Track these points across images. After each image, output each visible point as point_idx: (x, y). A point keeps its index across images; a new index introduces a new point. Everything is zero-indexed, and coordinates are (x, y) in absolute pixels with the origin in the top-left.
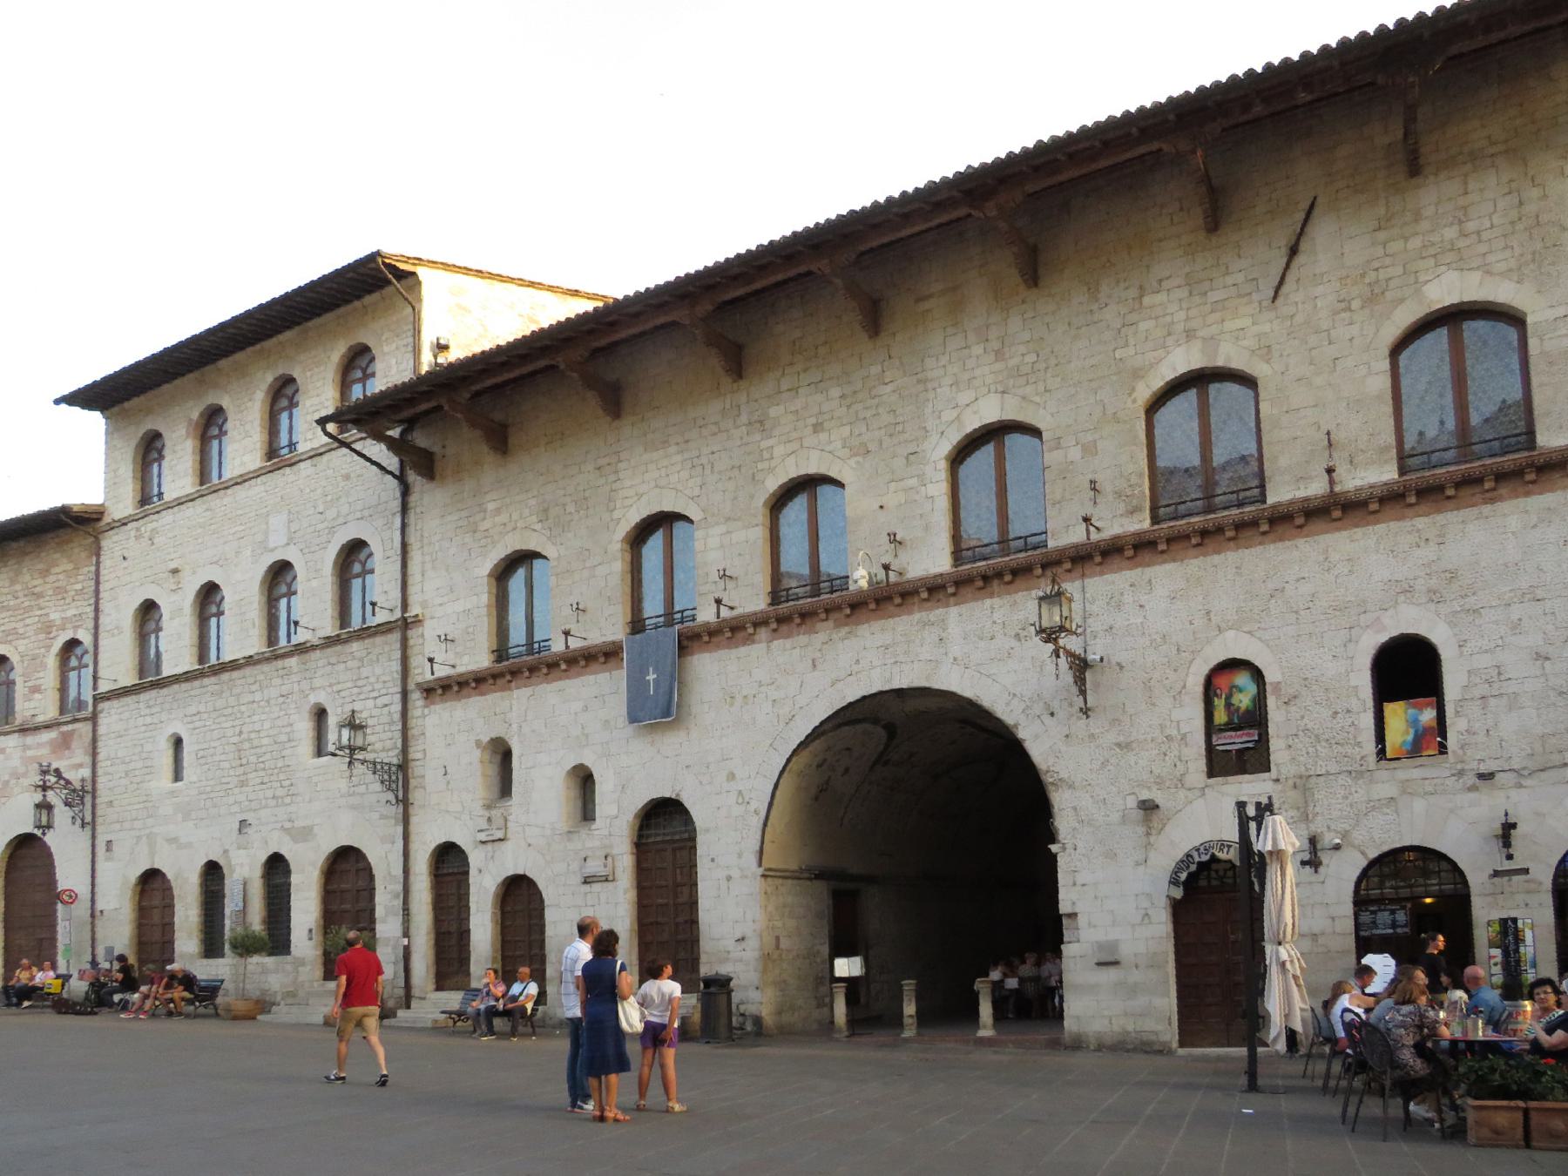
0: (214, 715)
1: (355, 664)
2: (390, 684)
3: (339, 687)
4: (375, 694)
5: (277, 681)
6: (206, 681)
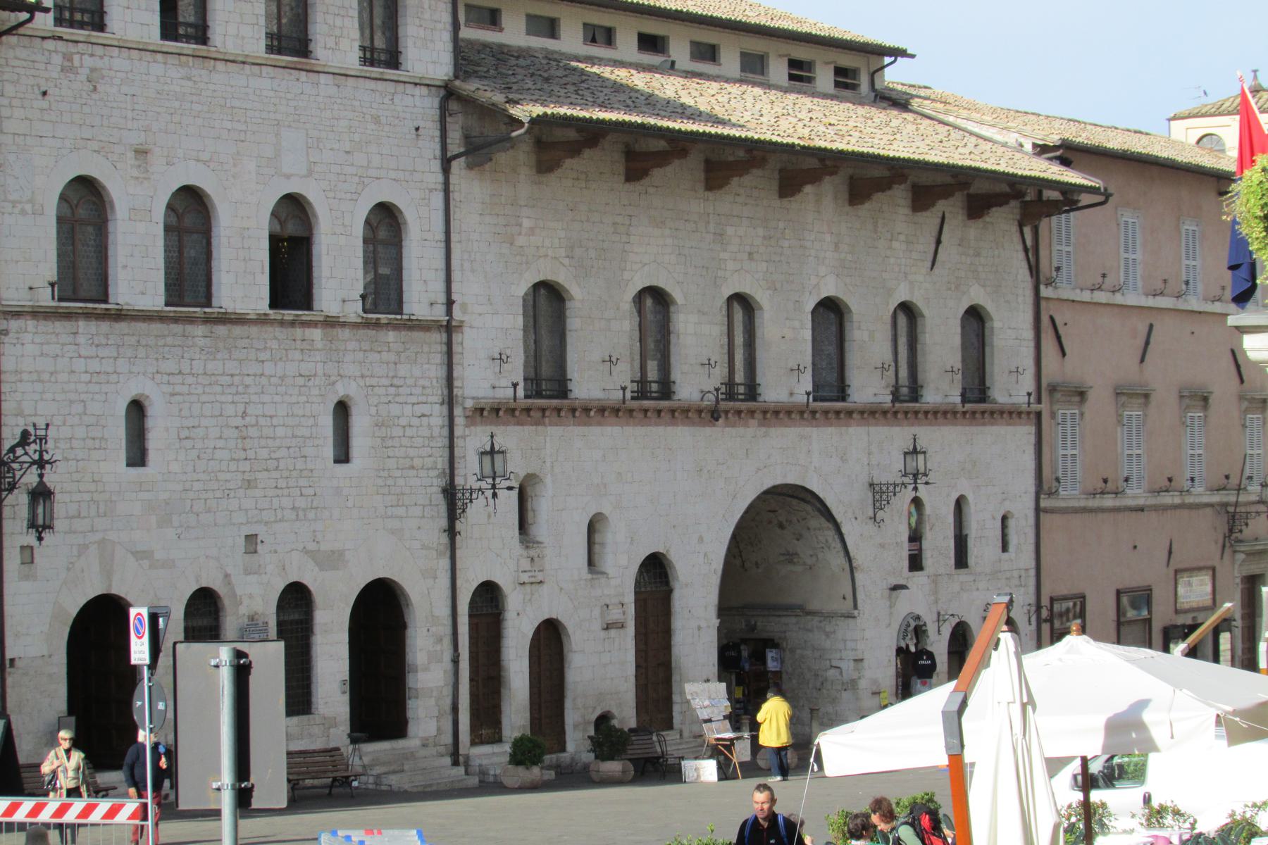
0: (206, 380)
1: (392, 357)
2: (428, 391)
3: (374, 381)
4: (414, 399)
5: (297, 355)
6: (189, 328)
